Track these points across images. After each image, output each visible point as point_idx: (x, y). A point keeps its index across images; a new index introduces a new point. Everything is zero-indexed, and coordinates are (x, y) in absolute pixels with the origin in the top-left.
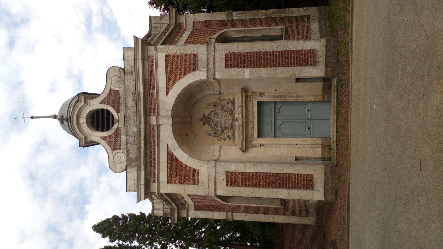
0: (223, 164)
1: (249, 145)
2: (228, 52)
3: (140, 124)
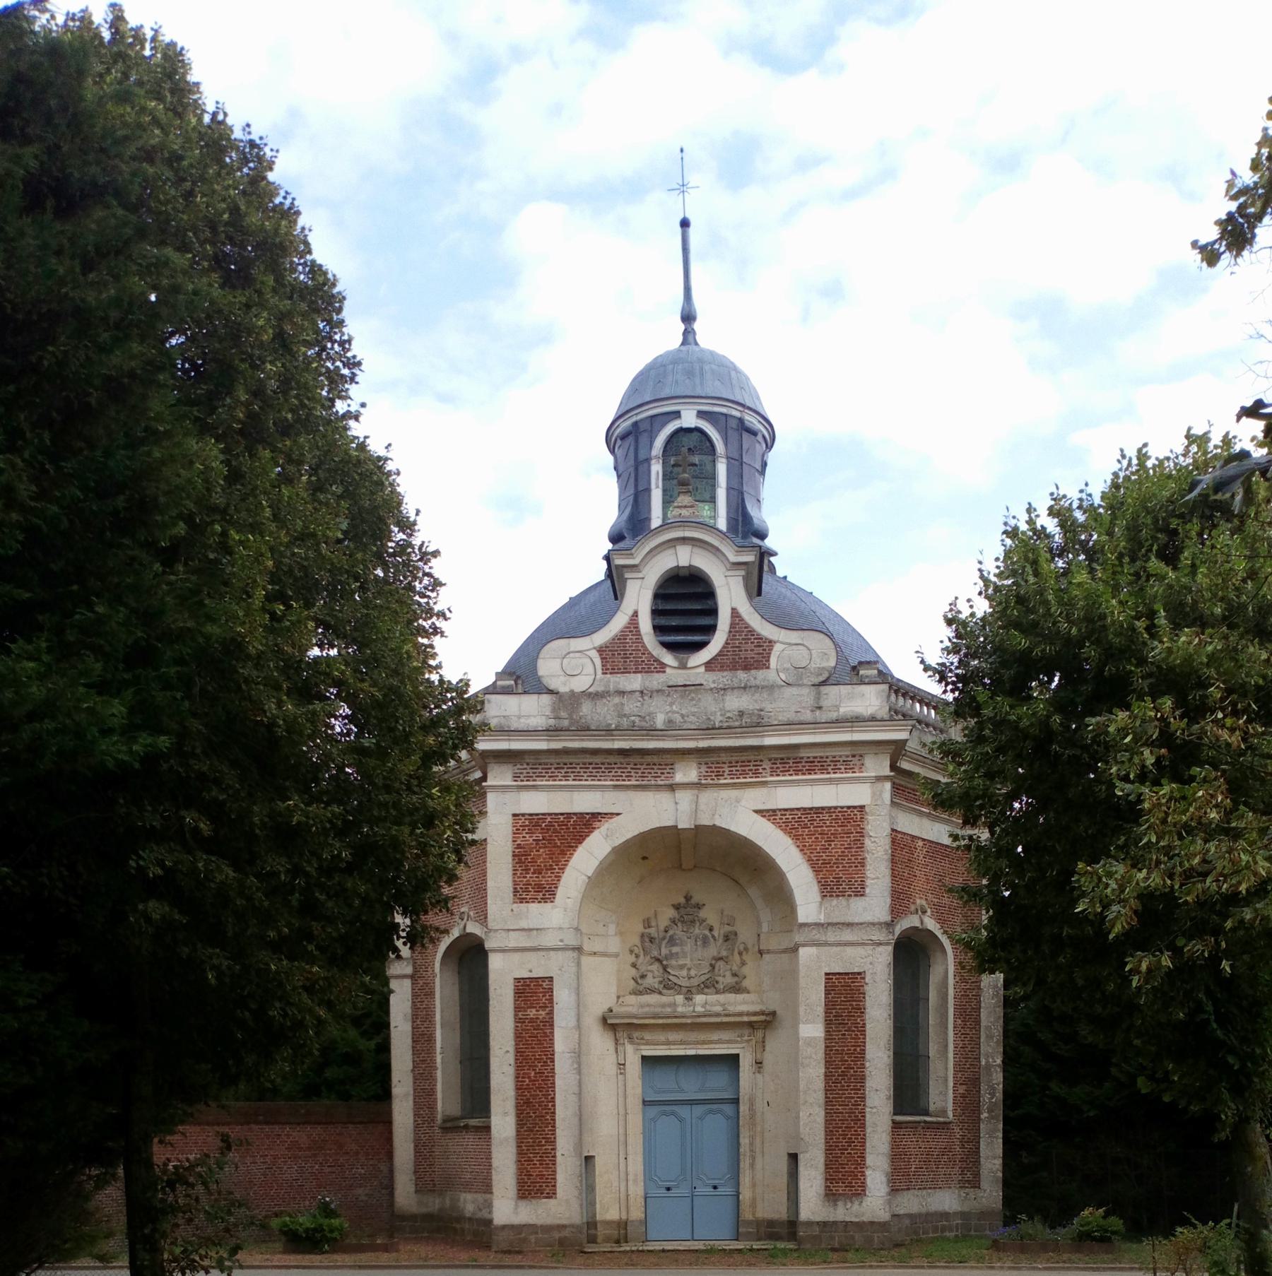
0: (574, 969)
1: (622, 1035)
2: (867, 980)
3: (676, 737)
